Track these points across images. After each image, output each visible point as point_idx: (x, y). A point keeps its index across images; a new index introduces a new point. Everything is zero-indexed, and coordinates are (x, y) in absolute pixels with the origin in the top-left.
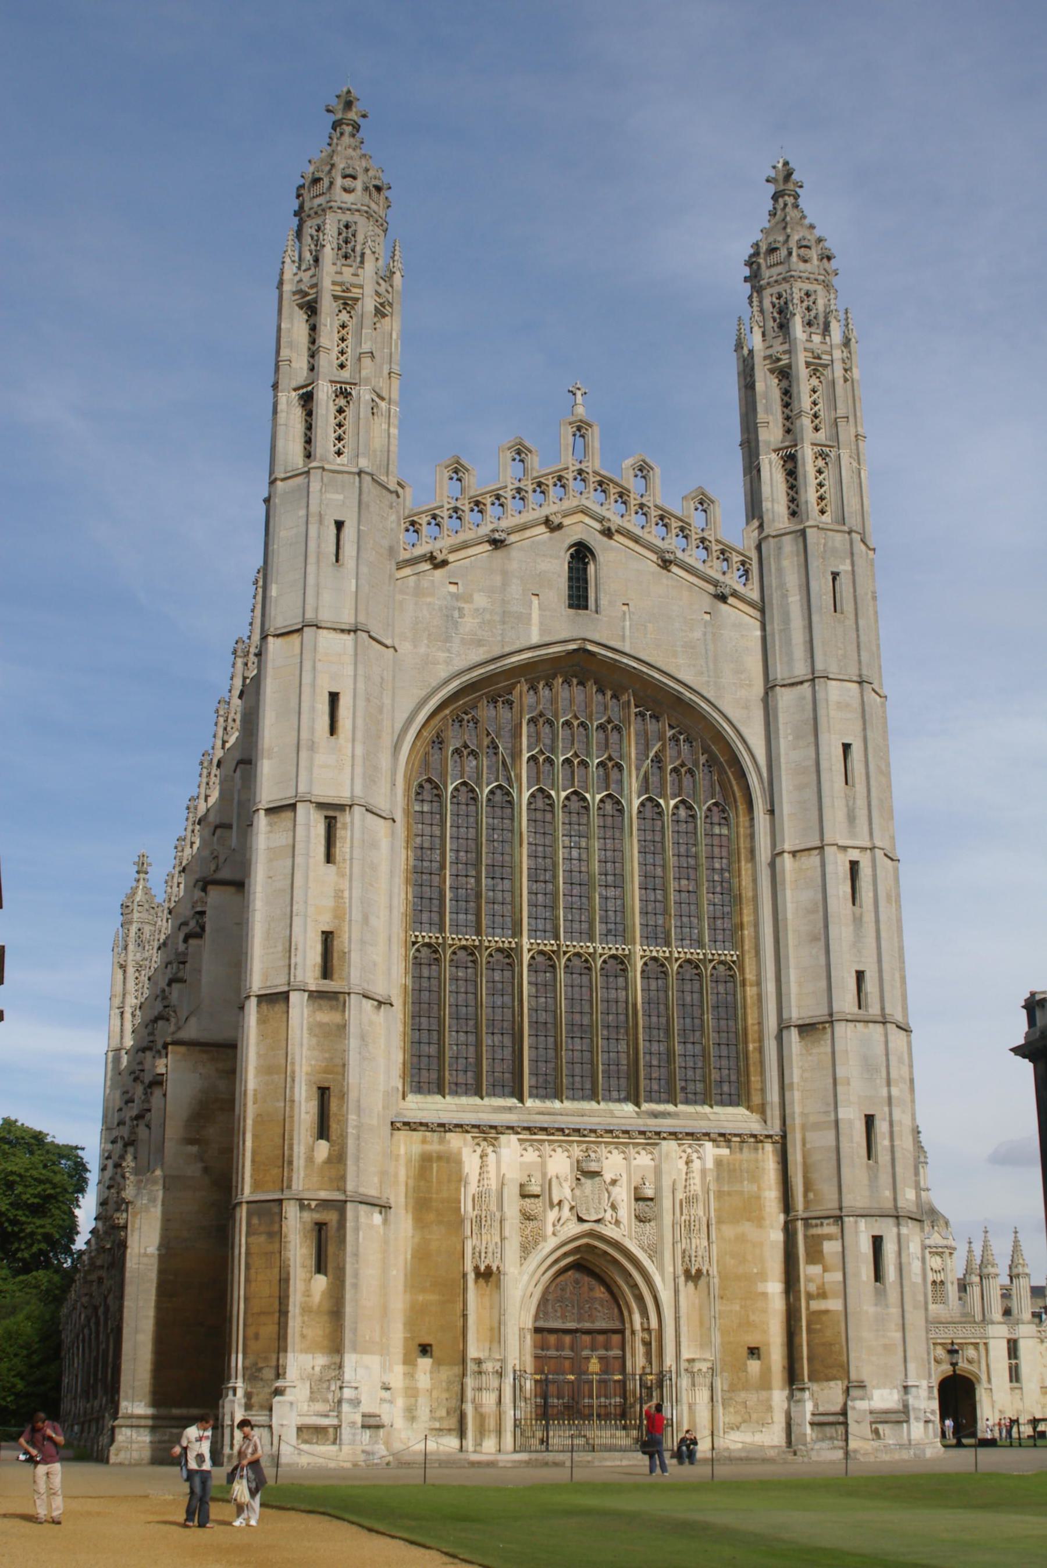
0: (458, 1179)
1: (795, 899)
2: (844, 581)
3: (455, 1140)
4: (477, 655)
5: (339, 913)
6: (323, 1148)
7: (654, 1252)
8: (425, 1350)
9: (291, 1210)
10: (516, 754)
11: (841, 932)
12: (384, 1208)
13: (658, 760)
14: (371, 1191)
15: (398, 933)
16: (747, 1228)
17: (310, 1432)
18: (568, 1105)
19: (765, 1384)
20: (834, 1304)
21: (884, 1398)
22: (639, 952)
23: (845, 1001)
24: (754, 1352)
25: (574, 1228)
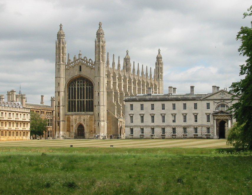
0: (70, 118)
3: (70, 116)
4: (72, 77)
8: (68, 131)
9: (56, 122)
13: (88, 84)
16: (91, 122)
18: (80, 112)
19: (92, 133)
21: (98, 135)
22: (85, 100)
25: (78, 122)
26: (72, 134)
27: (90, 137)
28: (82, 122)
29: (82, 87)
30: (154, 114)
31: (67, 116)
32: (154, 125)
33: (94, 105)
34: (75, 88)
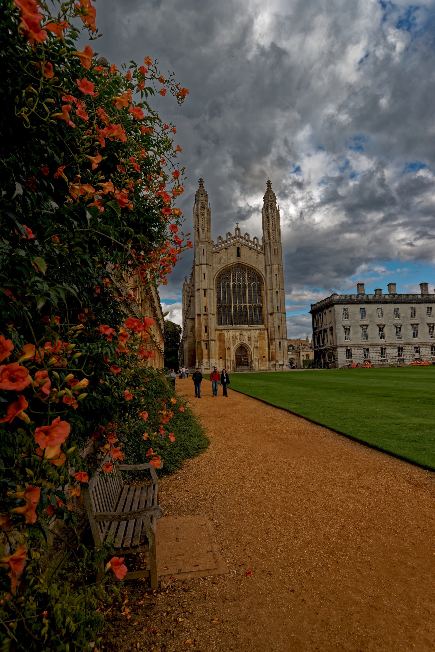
0: (224, 336)
1: (269, 296)
2: (276, 250)
3: (224, 331)
5: (207, 303)
6: (206, 334)
7: (251, 344)
8: (221, 358)
9: (202, 342)
10: (230, 278)
11: (275, 301)
12: (215, 341)
14: (213, 338)
15: (215, 304)
16: (263, 341)
17: (206, 369)
19: (266, 361)
20: (274, 351)
21: (281, 363)
22: (248, 305)
23: (276, 310)
24: (264, 357)
25: (240, 342)
26: (229, 364)
27: (262, 368)
28: (246, 342)
29: (241, 283)
30: (384, 325)
31: (218, 332)
32: (384, 342)
33: (265, 313)
34: (229, 285)
